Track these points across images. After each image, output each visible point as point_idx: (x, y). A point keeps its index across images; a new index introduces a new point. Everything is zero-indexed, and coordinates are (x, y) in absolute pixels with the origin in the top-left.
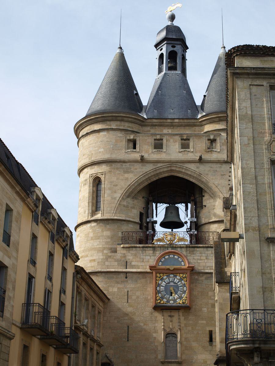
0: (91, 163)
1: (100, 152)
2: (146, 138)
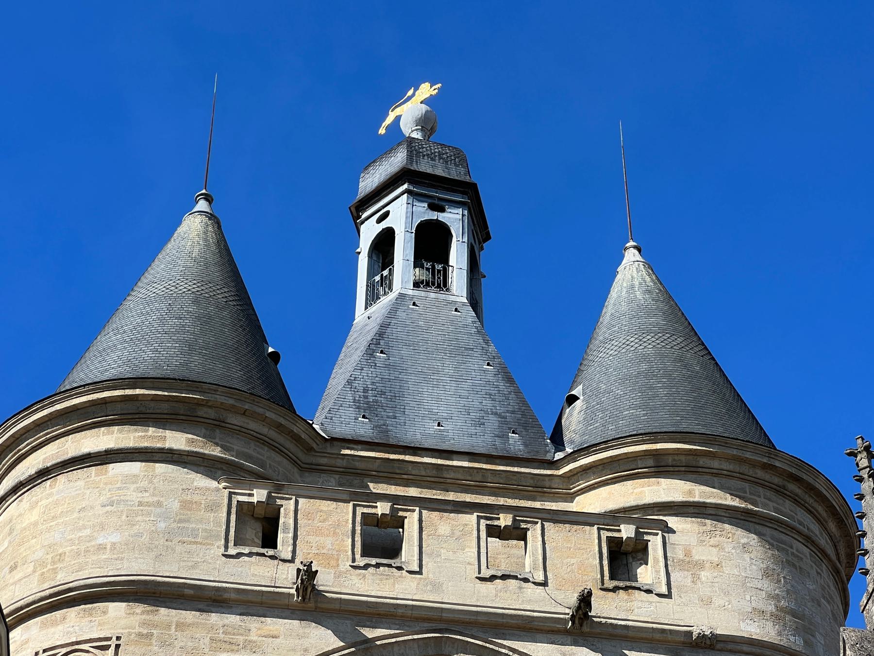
0: (51, 596)
1: (101, 548)
2: (325, 509)
